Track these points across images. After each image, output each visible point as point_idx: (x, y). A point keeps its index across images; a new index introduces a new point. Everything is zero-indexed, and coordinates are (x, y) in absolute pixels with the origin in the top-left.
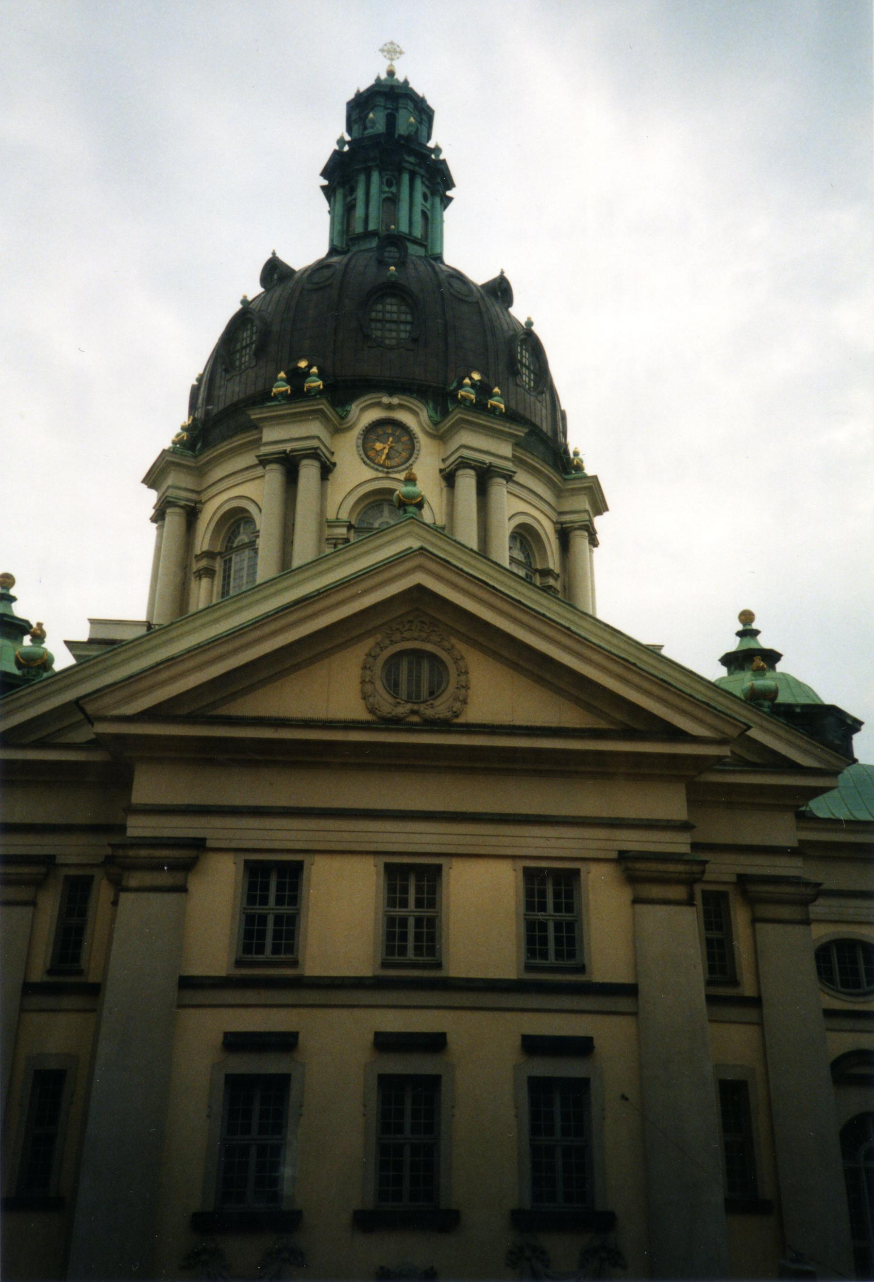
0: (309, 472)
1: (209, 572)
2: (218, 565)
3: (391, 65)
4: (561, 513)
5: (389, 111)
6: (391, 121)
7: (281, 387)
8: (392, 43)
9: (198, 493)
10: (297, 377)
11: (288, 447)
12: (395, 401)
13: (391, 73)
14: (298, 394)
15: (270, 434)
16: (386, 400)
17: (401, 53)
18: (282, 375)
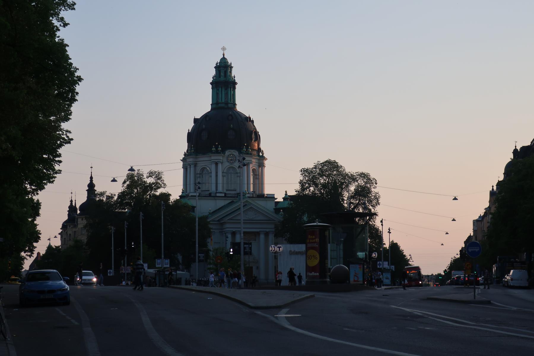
0: (220, 166)
1: (200, 177)
2: (201, 176)
3: (224, 53)
4: (259, 163)
5: (225, 70)
6: (226, 72)
7: (214, 149)
8: (224, 47)
9: (196, 162)
10: (217, 147)
11: (216, 161)
12: (233, 151)
13: (224, 55)
14: (217, 152)
15: (213, 158)
16: (231, 151)
17: (226, 49)
18: (214, 146)
